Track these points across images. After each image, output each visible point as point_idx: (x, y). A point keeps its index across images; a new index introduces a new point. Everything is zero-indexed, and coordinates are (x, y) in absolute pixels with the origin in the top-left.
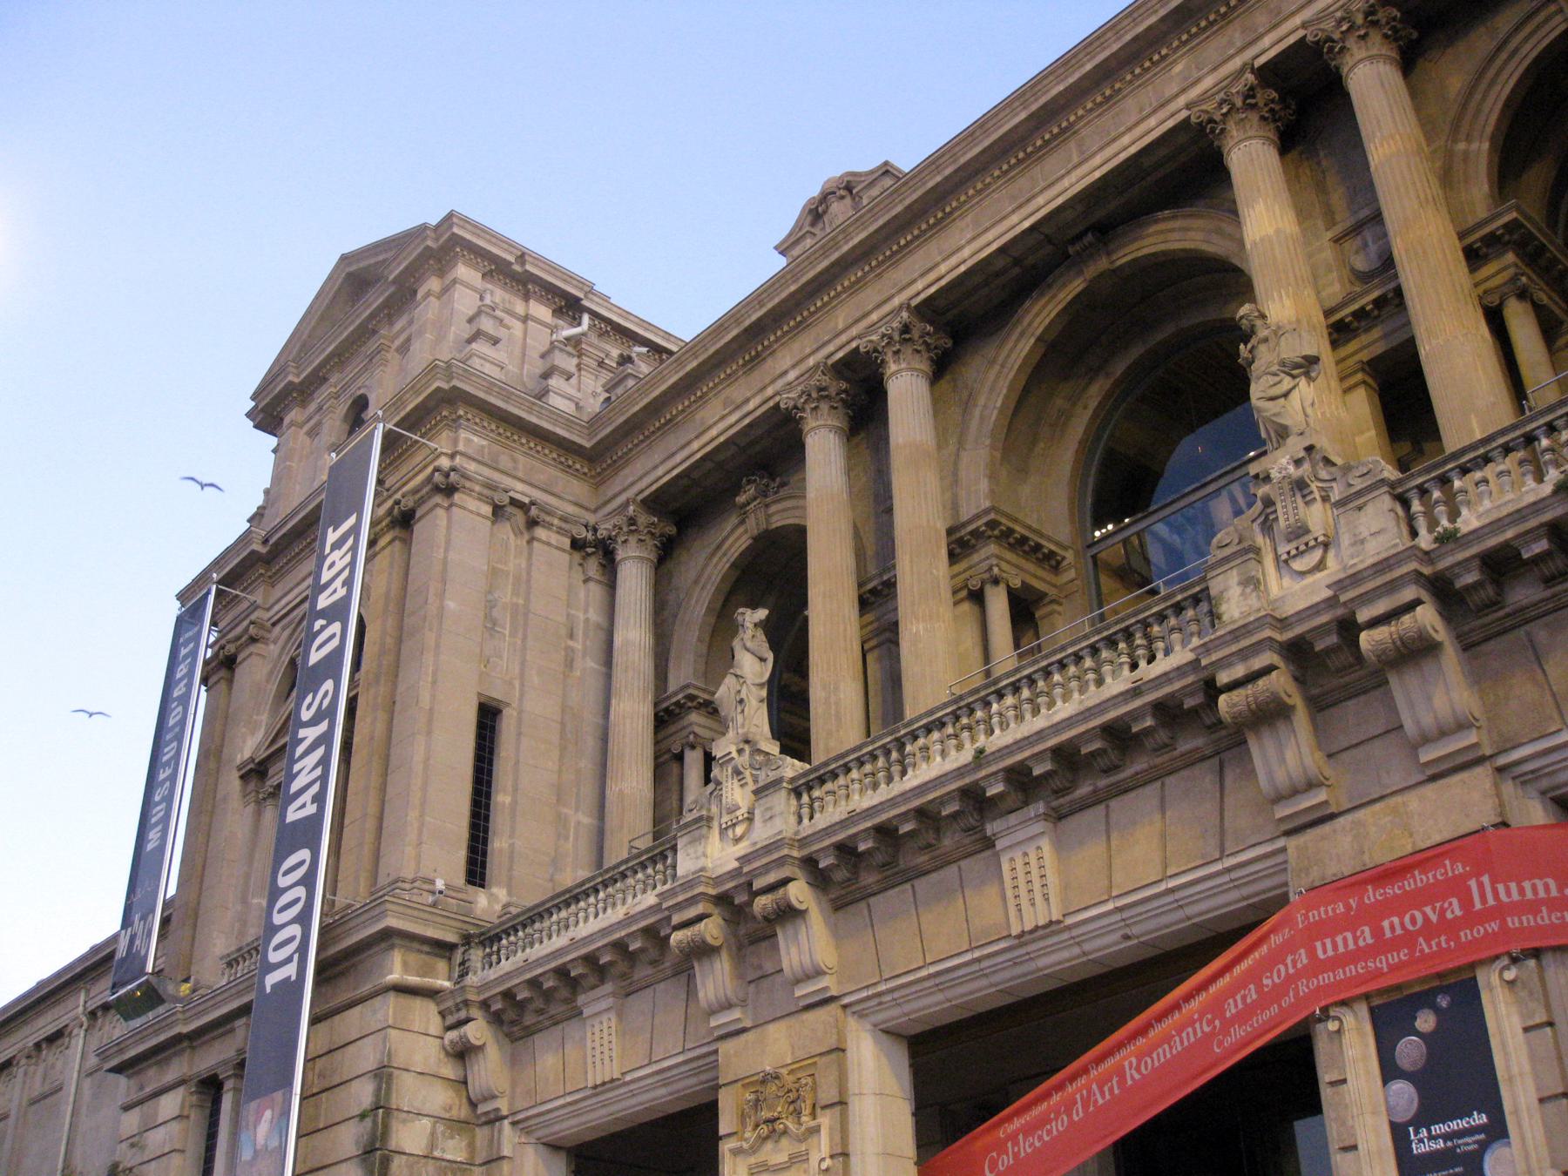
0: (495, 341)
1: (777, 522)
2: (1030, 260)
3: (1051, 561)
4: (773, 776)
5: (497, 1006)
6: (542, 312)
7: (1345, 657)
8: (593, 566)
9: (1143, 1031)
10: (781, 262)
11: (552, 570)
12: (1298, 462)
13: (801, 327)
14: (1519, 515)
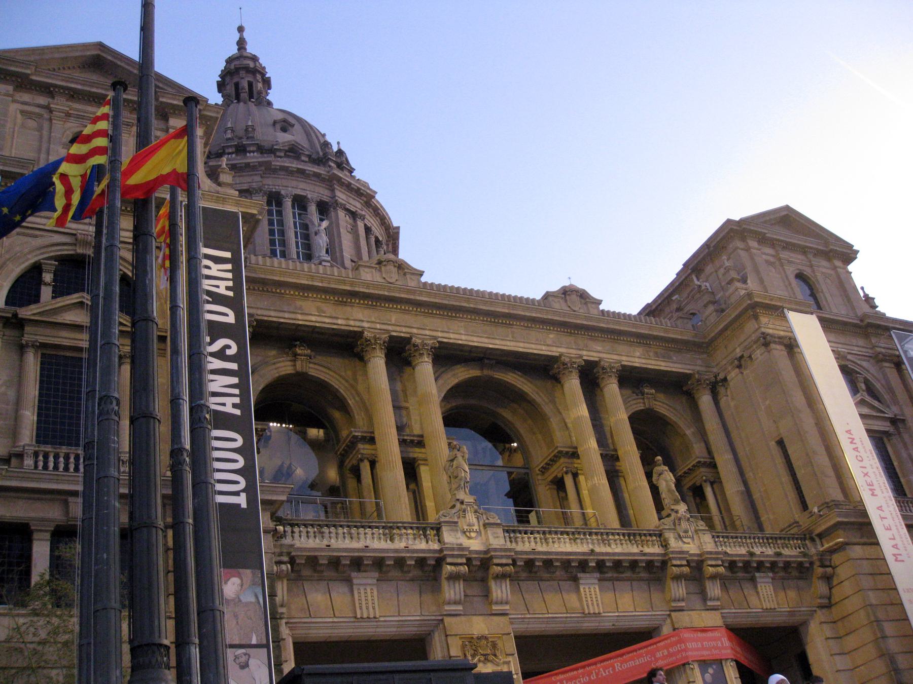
1: (312, 372)
4: (491, 521)
9: (622, 655)
14: (740, 555)
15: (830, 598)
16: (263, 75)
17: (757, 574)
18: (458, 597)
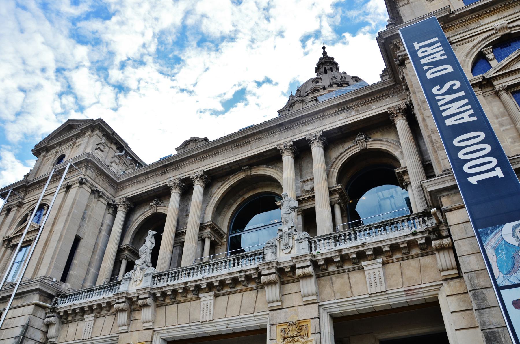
0: (102, 151)
1: (159, 211)
2: (233, 168)
3: (221, 236)
5: (61, 314)
6: (115, 148)
7: (291, 274)
8: (111, 211)
10: (175, 153)
11: (99, 208)
12: (289, 229)
13: (177, 168)
15: (459, 267)
16: (330, 62)
17: (363, 264)
18: (123, 322)
